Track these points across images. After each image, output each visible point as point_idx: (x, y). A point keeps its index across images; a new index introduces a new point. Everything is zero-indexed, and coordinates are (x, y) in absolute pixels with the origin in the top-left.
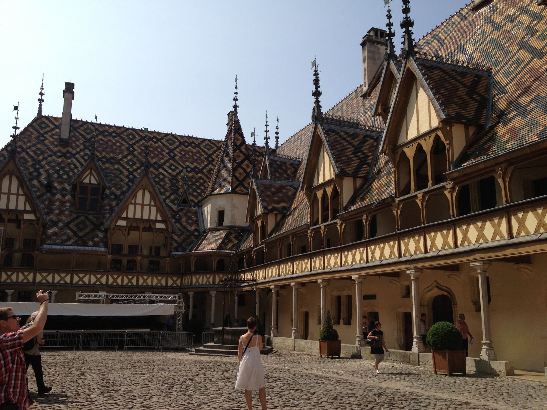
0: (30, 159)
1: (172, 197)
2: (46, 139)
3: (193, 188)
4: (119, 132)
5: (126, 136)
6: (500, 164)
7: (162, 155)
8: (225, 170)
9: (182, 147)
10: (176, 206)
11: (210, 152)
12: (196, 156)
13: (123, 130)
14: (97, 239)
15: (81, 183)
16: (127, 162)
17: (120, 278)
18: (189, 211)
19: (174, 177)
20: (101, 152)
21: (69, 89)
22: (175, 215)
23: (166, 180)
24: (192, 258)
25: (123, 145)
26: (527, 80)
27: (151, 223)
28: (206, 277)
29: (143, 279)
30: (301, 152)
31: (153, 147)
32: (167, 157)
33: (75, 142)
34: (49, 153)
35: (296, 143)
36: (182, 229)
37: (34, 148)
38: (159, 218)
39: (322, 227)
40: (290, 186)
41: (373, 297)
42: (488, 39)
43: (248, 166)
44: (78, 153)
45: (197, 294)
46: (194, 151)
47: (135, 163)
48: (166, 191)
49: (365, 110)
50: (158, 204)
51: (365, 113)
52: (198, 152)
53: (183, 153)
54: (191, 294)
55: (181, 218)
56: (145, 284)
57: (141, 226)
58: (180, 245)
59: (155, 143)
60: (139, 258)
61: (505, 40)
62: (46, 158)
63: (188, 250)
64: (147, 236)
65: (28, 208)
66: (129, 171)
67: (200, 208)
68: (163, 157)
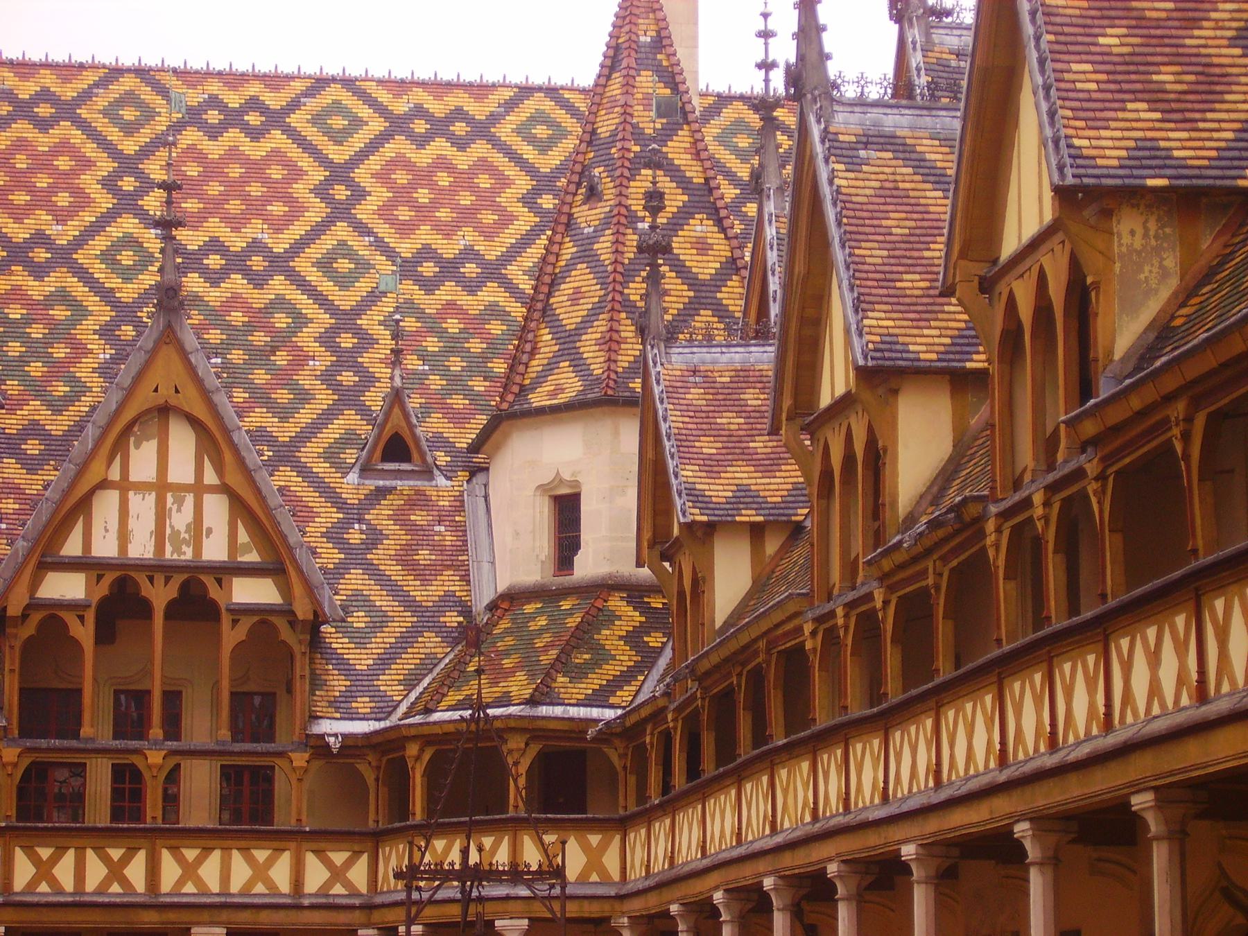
1: (333, 432)
3: (445, 373)
4: (69, 92)
5: (105, 113)
6: (1169, 398)
7: (289, 200)
8: (582, 277)
10: (353, 477)
12: (474, 189)
13: (91, 77)
16: (108, 257)
17: (69, 857)
18: (419, 500)
19: (346, 319)
22: (345, 525)
23: (307, 339)
24: (412, 749)
25: (86, 164)
27: (209, 581)
29: (181, 860)
31: (246, 161)
32: (316, 211)
36: (382, 601)
39: (840, 612)
43: (702, 247)
46: (463, 161)
48: (304, 397)
53: (401, 178)
55: (374, 538)
56: (189, 888)
57: (160, 595)
58: (362, 683)
59: (256, 134)
63: (403, 708)
66: (115, 304)
67: (480, 478)
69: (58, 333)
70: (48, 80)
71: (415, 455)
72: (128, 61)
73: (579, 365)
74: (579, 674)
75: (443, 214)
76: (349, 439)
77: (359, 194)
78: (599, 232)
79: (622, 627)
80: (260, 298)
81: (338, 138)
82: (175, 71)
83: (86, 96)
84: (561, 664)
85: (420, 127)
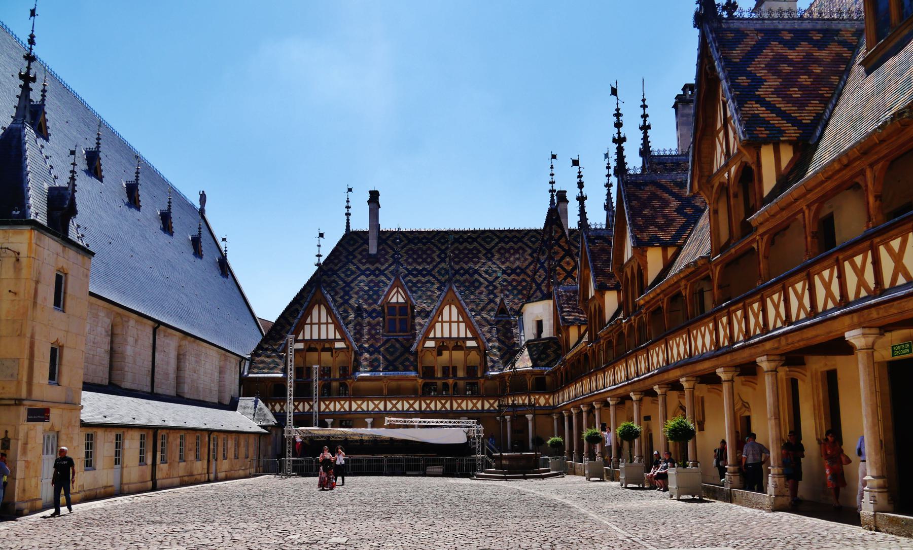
0: (340, 283)
2: (355, 257)
14: (407, 363)
18: (509, 323)
19: (491, 283)
20: (410, 264)
21: (374, 197)
33: (383, 256)
34: (359, 273)
37: (344, 270)
38: (469, 335)
43: (568, 263)
44: (387, 268)
46: (516, 247)
52: (521, 248)
59: (470, 243)
62: (356, 278)
64: (458, 355)
65: (338, 337)
74: (542, 360)
77: (493, 256)
79: (553, 349)
80: (471, 279)
81: (488, 243)
84: (539, 358)
85: (507, 240)
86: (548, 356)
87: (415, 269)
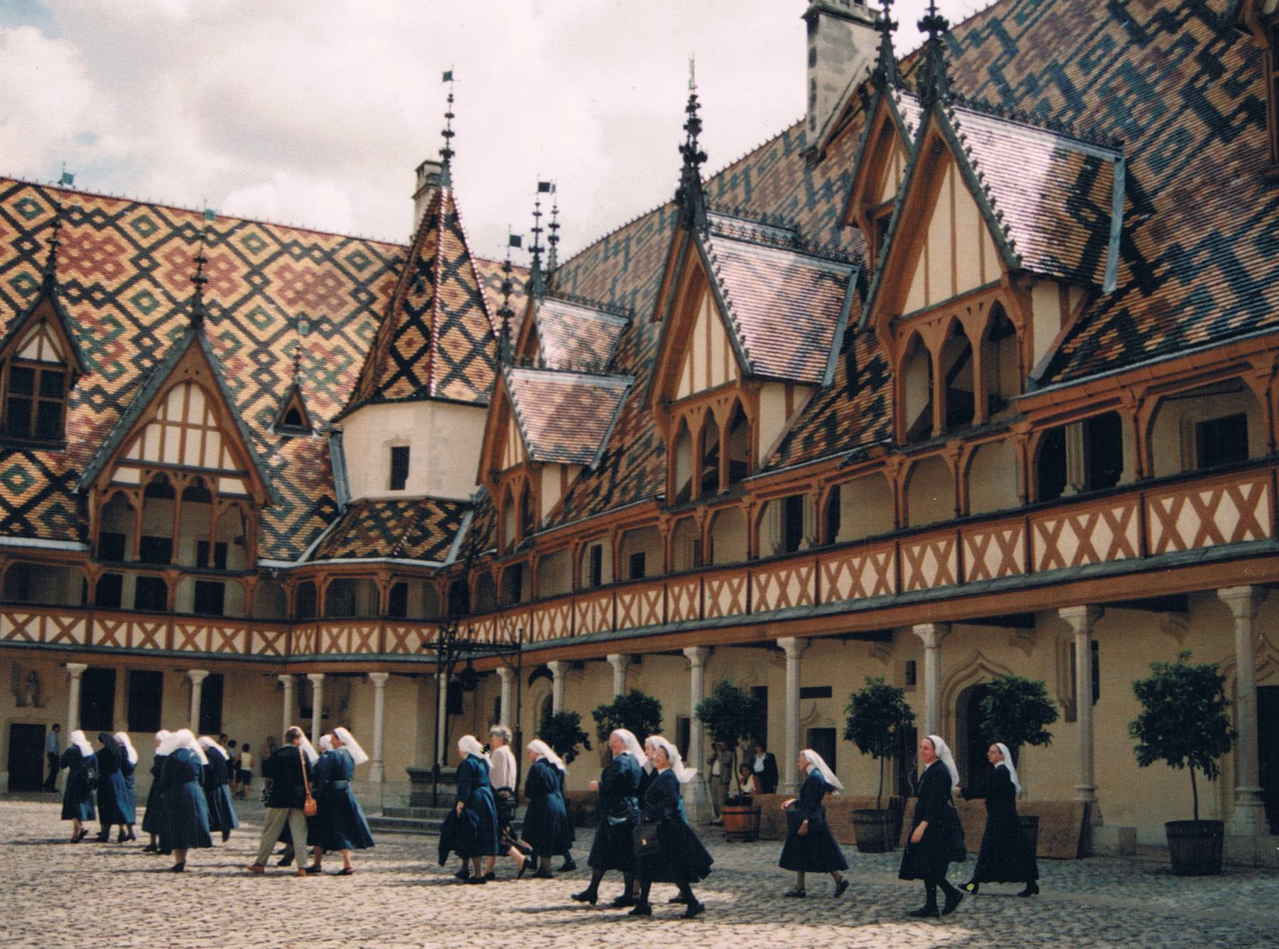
4: (111, 211)
7: (230, 281)
9: (285, 259)
11: (364, 276)
12: (325, 286)
13: (124, 205)
15: (15, 358)
16: (135, 300)
17: (124, 628)
19: (264, 346)
23: (243, 355)
24: (321, 576)
25: (122, 250)
26: (1197, 190)
27: (206, 478)
28: (360, 633)
29: (185, 632)
30: (630, 288)
35: (612, 261)
38: (229, 465)
40: (603, 389)
41: (826, 692)
42: (1118, 65)
45: (331, 677)
47: (156, 304)
48: (242, 385)
49: (811, 194)
50: (228, 424)
51: (812, 203)
52: (329, 274)
53: (288, 276)
54: (316, 678)
56: (189, 648)
58: (283, 540)
60: (174, 574)
61: (1155, 75)
68: (233, 288)
69: (110, 338)
70: (100, 204)
71: (304, 422)
72: (142, 199)
73: (414, 380)
74: (415, 541)
75: (311, 297)
76: (269, 410)
77: (267, 282)
78: (423, 310)
82: (167, 207)
83: (121, 215)
85: (296, 251)
86: (427, 534)
87: (74, 284)
